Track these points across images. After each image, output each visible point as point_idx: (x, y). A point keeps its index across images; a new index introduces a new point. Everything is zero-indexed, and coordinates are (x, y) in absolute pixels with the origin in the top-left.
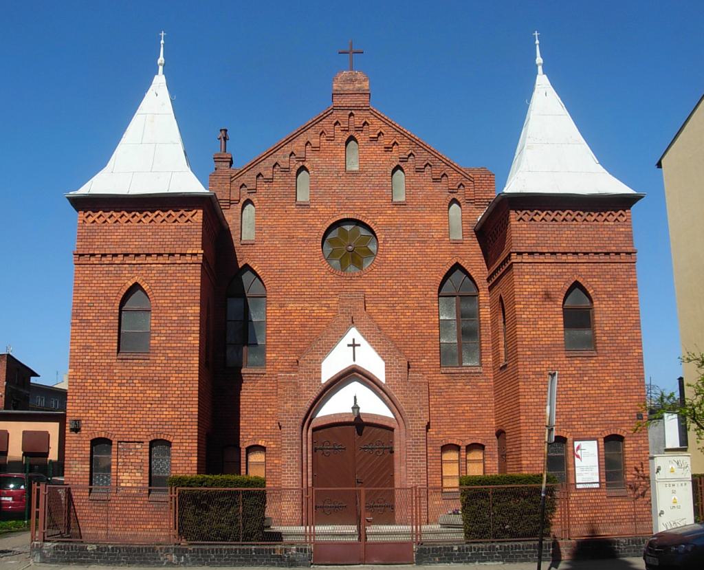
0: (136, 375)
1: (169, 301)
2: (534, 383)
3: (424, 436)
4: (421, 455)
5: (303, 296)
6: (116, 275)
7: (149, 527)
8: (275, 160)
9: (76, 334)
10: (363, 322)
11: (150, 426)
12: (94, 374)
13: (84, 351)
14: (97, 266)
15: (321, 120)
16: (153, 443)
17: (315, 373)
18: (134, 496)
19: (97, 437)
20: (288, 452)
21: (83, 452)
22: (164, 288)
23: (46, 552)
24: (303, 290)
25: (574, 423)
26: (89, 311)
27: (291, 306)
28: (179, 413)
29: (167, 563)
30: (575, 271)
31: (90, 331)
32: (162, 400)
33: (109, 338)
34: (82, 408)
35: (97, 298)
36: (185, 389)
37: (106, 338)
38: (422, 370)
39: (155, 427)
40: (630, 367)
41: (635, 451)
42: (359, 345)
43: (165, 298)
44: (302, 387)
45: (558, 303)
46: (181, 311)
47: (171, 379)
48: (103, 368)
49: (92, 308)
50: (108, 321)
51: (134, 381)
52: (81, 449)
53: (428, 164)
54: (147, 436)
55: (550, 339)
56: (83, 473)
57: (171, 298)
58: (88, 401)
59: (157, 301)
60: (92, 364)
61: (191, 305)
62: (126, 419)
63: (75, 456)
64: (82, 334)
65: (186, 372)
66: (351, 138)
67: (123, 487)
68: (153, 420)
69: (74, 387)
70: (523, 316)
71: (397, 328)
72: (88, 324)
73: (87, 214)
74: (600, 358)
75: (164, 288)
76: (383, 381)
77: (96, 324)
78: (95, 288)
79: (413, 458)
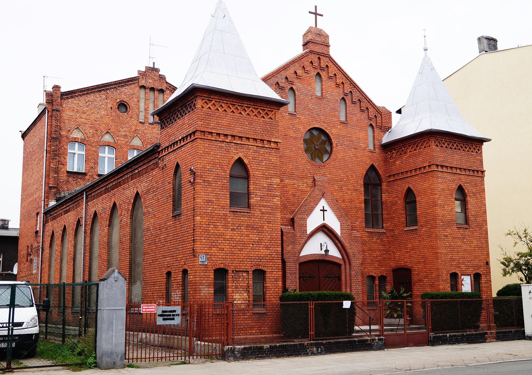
0: (243, 223)
1: (261, 173)
2: (444, 241)
3: (360, 270)
4: (359, 282)
5: (293, 176)
6: (226, 150)
8: (276, 80)
10: (328, 196)
11: (252, 260)
12: (215, 221)
14: (213, 141)
15: (302, 58)
16: (255, 271)
17: (304, 227)
18: (243, 310)
20: (290, 279)
21: (209, 279)
22: (258, 163)
24: (293, 172)
26: (209, 175)
27: (287, 181)
28: (270, 251)
30: (460, 179)
31: (211, 189)
32: (259, 242)
34: (207, 246)
35: (215, 166)
36: (273, 234)
37: (222, 195)
38: (356, 229)
39: (256, 260)
40: (483, 236)
41: (486, 283)
42: (326, 211)
43: (259, 171)
46: (269, 181)
47: (265, 227)
48: (221, 217)
52: (207, 276)
53: (359, 99)
54: (249, 266)
56: (210, 295)
60: (213, 214)
63: (203, 282)
64: (205, 191)
65: (273, 223)
66: (318, 74)
67: (235, 304)
68: (255, 255)
69: (201, 231)
70: (439, 202)
71: (343, 201)
72: (210, 184)
73: (204, 101)
74: (471, 229)
75: (258, 163)
76: (340, 235)
77: (214, 185)
78: (213, 158)
79: (355, 284)
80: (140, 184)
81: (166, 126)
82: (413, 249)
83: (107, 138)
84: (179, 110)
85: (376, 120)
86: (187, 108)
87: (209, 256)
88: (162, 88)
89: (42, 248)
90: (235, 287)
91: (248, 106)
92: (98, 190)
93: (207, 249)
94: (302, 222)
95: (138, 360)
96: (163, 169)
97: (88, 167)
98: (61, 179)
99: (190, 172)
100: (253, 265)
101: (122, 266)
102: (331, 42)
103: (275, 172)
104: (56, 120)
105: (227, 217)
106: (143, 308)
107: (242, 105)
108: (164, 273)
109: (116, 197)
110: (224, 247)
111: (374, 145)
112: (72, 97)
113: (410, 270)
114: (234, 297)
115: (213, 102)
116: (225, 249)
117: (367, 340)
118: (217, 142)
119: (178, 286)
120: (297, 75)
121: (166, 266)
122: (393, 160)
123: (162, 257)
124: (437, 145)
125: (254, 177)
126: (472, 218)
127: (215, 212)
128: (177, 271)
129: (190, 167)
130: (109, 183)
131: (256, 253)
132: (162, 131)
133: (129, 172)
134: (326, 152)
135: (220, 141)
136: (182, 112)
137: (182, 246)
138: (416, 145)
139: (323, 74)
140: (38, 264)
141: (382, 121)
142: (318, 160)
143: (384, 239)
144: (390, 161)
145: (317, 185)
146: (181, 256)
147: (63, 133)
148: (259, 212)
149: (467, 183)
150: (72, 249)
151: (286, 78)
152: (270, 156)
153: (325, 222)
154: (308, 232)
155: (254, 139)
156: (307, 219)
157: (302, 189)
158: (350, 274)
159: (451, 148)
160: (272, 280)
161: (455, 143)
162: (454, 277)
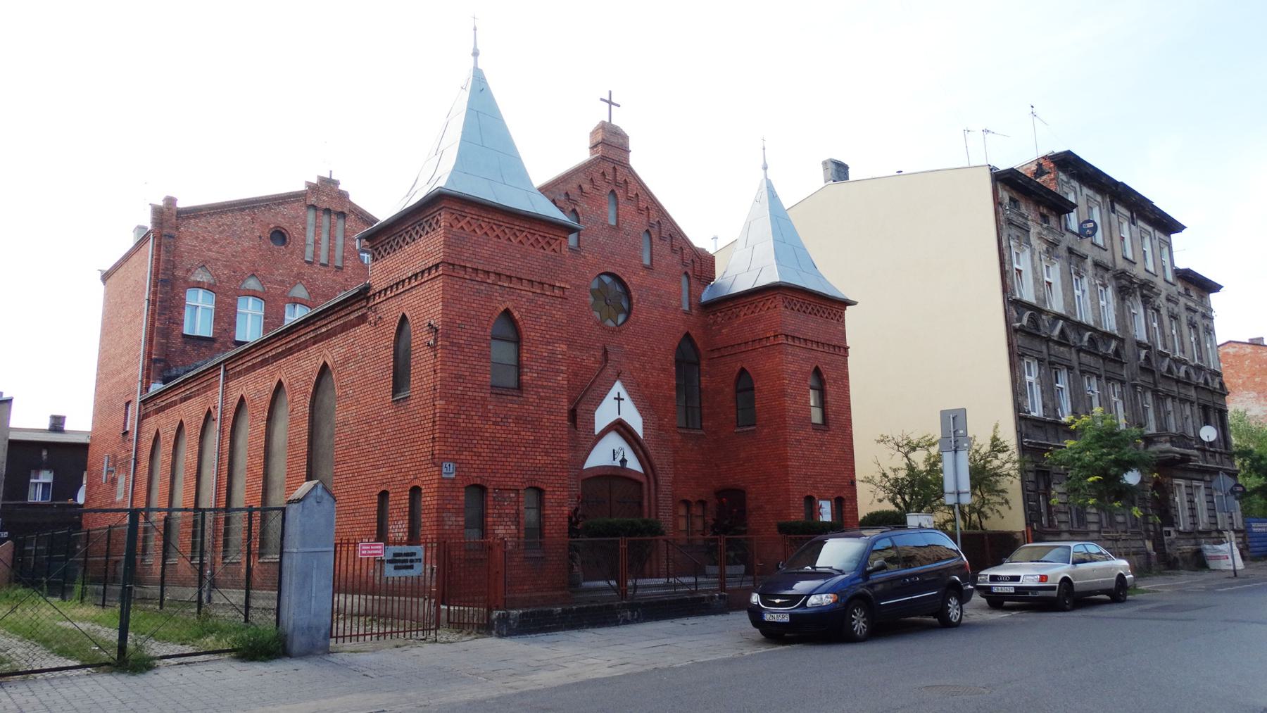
0: (510, 413)
1: (539, 335)
4: (669, 509)
6: (487, 296)
7: (526, 587)
9: (447, 359)
11: (524, 472)
13: (455, 380)
14: (467, 281)
19: (472, 483)
21: (458, 502)
23: (512, 622)
25: (819, 485)
26: (461, 333)
29: (624, 620)
31: (462, 357)
33: (483, 368)
39: (529, 473)
42: (623, 399)
44: (580, 437)
45: (808, 383)
46: (550, 348)
49: (463, 330)
50: (480, 348)
51: (509, 420)
56: (458, 528)
58: (462, 441)
59: (529, 333)
61: (559, 342)
62: (502, 463)
63: (448, 506)
66: (613, 191)
68: (528, 465)
69: (446, 423)
70: (789, 391)
72: (460, 349)
73: (454, 217)
74: (831, 433)
76: (642, 437)
79: (664, 512)
80: (330, 349)
81: (383, 257)
83: (252, 284)
84: (409, 231)
85: (694, 267)
86: (424, 227)
87: (458, 465)
88: (344, 210)
89: (135, 459)
90: (497, 515)
91: (521, 228)
92: (249, 360)
93: (454, 453)
94: (588, 416)
95: (353, 638)
96: (375, 325)
97: (219, 329)
98: (173, 347)
99: (428, 328)
100: (525, 480)
101: (293, 485)
102: (632, 145)
104: (167, 252)
105: (486, 403)
106: (362, 550)
107: (512, 226)
108: (374, 494)
109: (283, 373)
110: (482, 450)
111: (690, 304)
112: (196, 217)
113: (744, 492)
114: (496, 531)
115: (468, 219)
116: (483, 454)
117: (704, 598)
118: (474, 283)
119: (402, 514)
120: (582, 192)
121: (379, 482)
122: (718, 327)
123: (371, 468)
124: (786, 307)
125: (528, 340)
126: (833, 416)
127: (469, 393)
128: (400, 490)
129: (428, 320)
130: (271, 350)
131: (531, 461)
132: (374, 264)
133: (310, 332)
134: (622, 311)
135: (477, 281)
136: (420, 230)
137: (411, 449)
138: (754, 305)
139: (620, 193)
140: (126, 486)
141: (701, 268)
142: (610, 323)
143: (703, 445)
144: (714, 328)
145: (611, 360)
146: (408, 465)
147: (179, 273)
148: (535, 397)
149: (826, 364)
150: (193, 459)
151: (567, 194)
152: (552, 308)
153: (620, 417)
154: (596, 433)
155: (528, 280)
156: (595, 411)
157: (588, 364)
158: (657, 498)
159: (804, 312)
160: (554, 504)
161: (810, 305)
162: (811, 503)
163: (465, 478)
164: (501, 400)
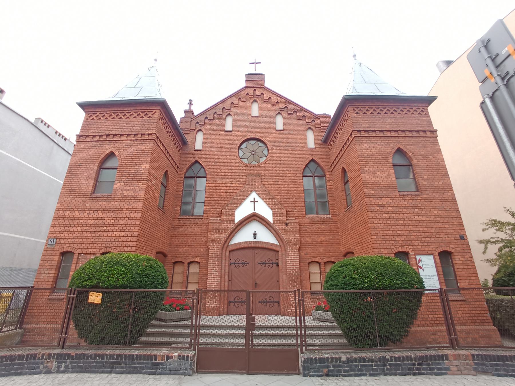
1: (130, 161)
32: (116, 223)
45: (389, 161)
46: (137, 167)
55: (386, 183)
57: (132, 160)
61: (144, 163)
70: (365, 169)
74: (424, 196)
82: (352, 229)
103: (146, 159)
105: (85, 203)
126: (426, 183)
163: (61, 247)
164: (96, 201)
